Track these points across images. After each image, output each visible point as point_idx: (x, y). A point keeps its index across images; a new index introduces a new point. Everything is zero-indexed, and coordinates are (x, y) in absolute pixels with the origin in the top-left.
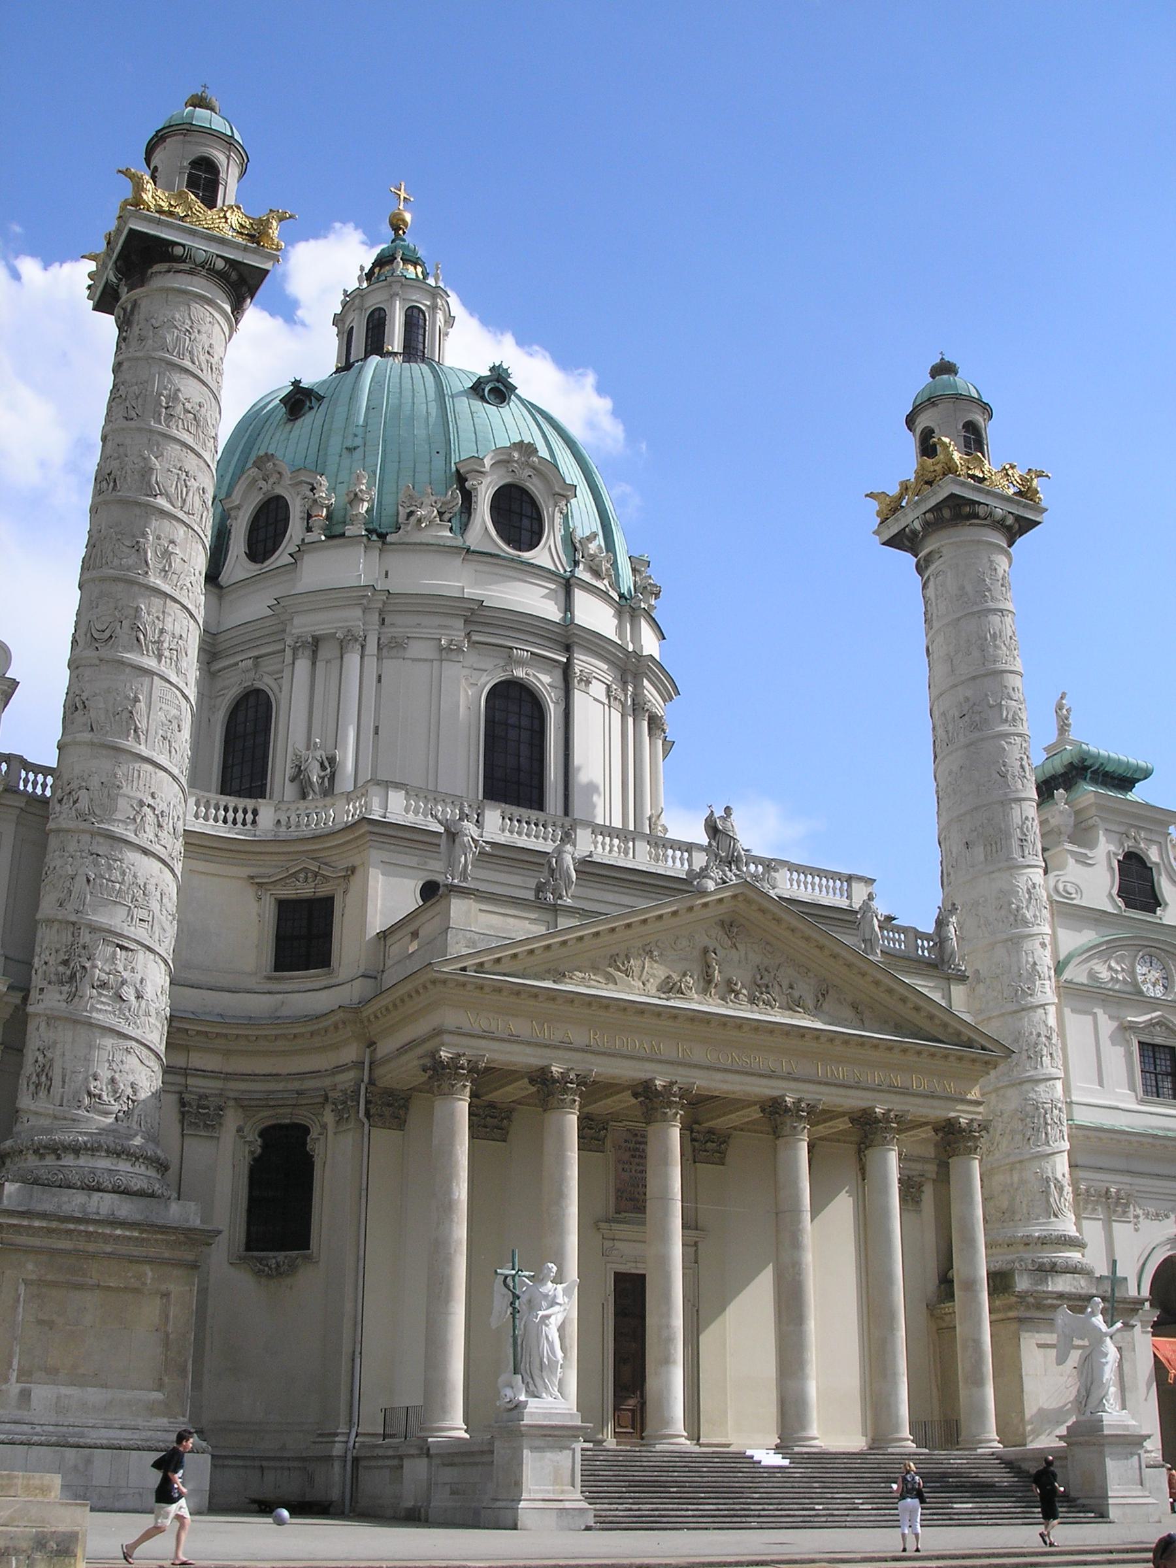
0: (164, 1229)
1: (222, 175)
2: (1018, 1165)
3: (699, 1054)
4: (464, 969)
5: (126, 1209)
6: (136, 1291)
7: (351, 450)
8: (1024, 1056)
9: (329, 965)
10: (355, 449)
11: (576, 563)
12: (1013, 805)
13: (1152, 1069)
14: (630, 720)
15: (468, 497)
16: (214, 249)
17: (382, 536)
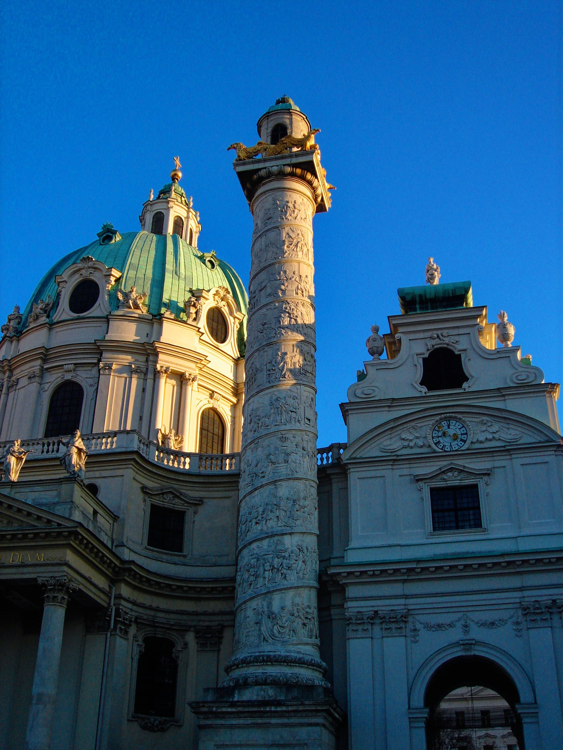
2: (243, 606)
8: (254, 521)
11: (118, 307)
14: (150, 382)
15: (59, 295)
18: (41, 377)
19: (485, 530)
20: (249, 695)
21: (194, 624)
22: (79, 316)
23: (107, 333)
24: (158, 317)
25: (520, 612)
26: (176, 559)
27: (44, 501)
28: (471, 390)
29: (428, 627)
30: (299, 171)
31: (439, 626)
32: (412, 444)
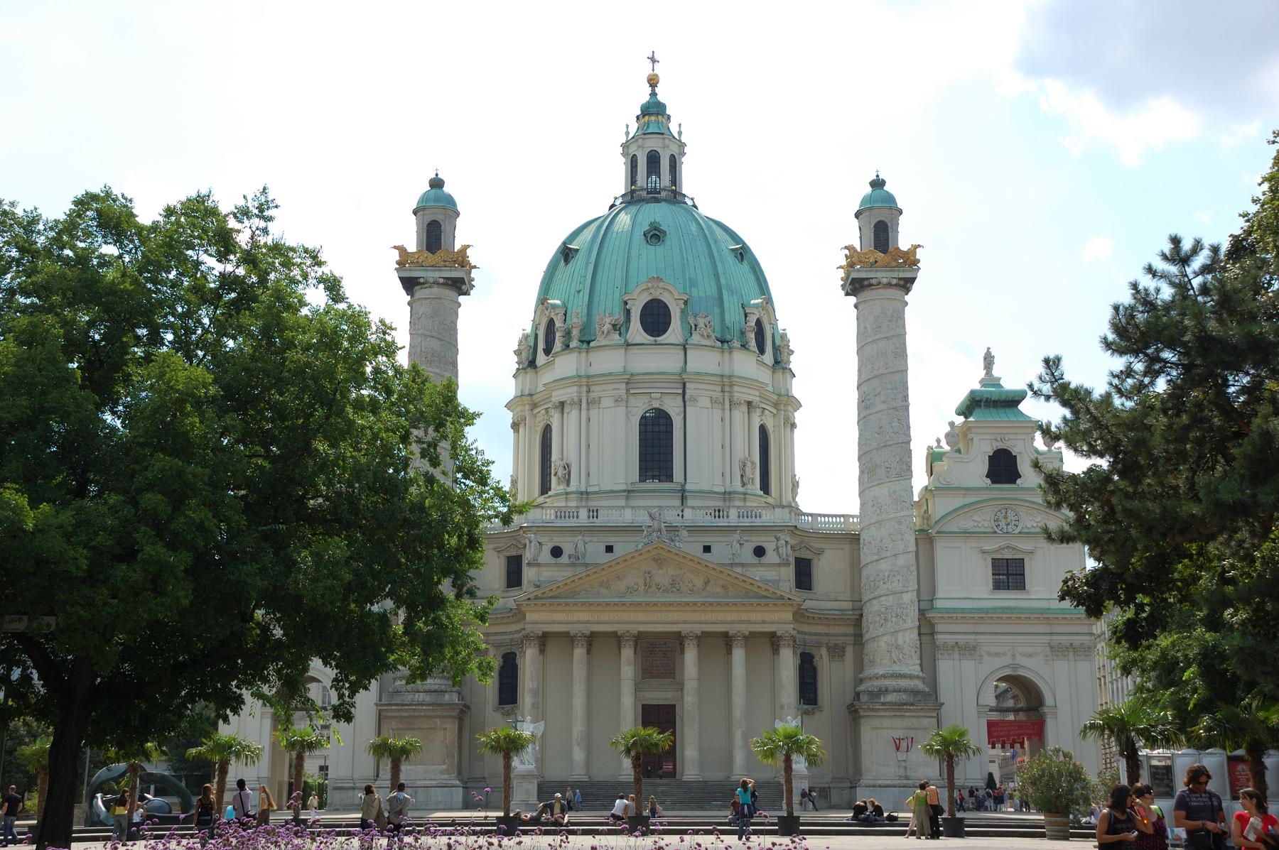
0: (440, 705)
1: (443, 227)
3: (641, 617)
4: (529, 599)
5: (428, 698)
6: (434, 729)
7: (579, 292)
8: (882, 581)
9: (521, 585)
10: (579, 292)
11: (691, 334)
12: (883, 449)
13: (1005, 572)
14: (727, 412)
15: (628, 312)
16: (437, 274)
17: (589, 342)
18: (627, 402)
19: (1028, 592)
20: (891, 698)
21: (825, 642)
22: (655, 341)
23: (686, 362)
24: (726, 344)
25: (1048, 649)
26: (810, 596)
27: (769, 578)
28: (1025, 485)
29: (989, 654)
30: (902, 283)
31: (997, 654)
32: (980, 525)
